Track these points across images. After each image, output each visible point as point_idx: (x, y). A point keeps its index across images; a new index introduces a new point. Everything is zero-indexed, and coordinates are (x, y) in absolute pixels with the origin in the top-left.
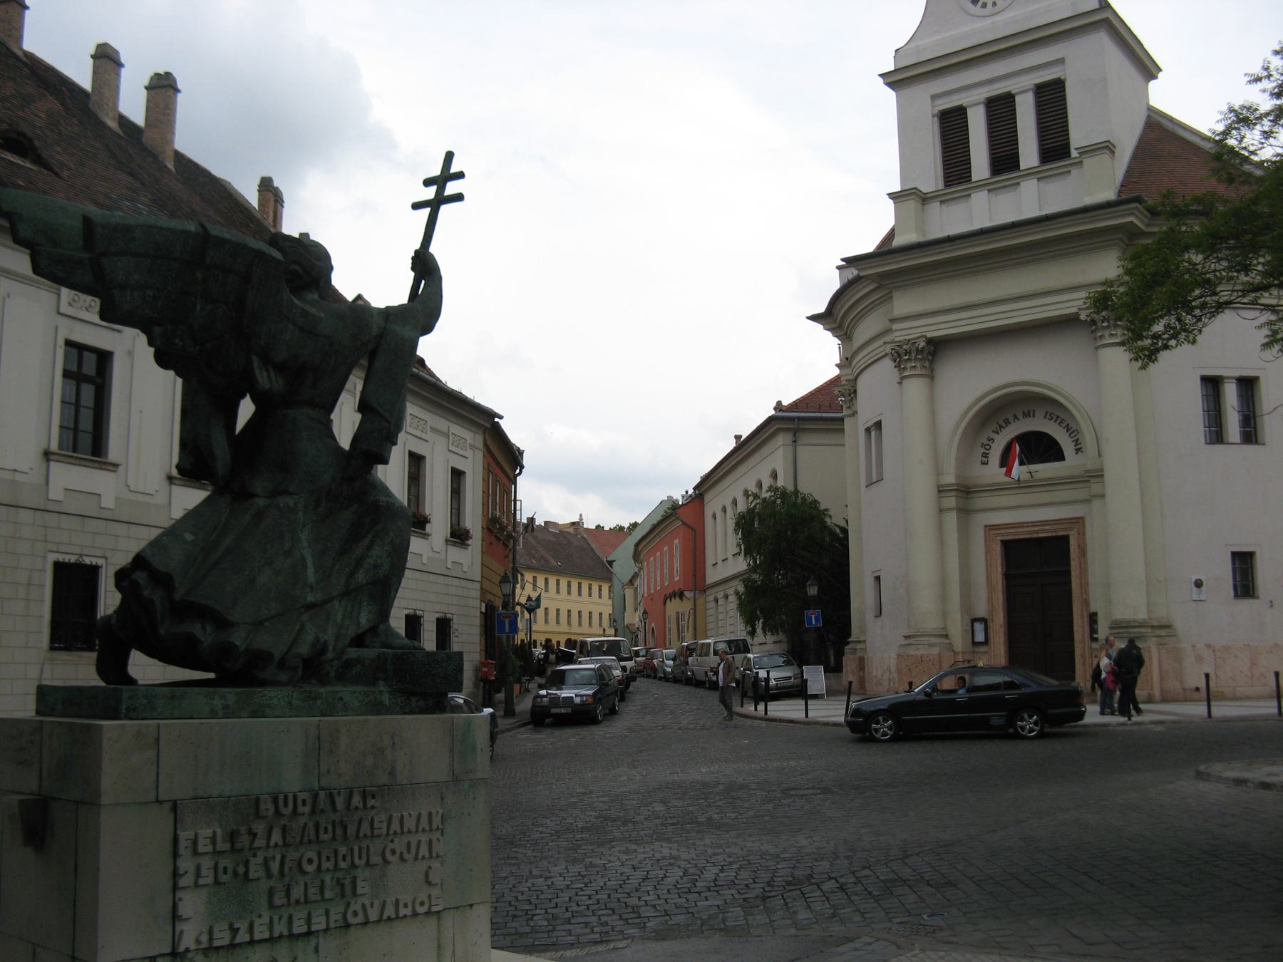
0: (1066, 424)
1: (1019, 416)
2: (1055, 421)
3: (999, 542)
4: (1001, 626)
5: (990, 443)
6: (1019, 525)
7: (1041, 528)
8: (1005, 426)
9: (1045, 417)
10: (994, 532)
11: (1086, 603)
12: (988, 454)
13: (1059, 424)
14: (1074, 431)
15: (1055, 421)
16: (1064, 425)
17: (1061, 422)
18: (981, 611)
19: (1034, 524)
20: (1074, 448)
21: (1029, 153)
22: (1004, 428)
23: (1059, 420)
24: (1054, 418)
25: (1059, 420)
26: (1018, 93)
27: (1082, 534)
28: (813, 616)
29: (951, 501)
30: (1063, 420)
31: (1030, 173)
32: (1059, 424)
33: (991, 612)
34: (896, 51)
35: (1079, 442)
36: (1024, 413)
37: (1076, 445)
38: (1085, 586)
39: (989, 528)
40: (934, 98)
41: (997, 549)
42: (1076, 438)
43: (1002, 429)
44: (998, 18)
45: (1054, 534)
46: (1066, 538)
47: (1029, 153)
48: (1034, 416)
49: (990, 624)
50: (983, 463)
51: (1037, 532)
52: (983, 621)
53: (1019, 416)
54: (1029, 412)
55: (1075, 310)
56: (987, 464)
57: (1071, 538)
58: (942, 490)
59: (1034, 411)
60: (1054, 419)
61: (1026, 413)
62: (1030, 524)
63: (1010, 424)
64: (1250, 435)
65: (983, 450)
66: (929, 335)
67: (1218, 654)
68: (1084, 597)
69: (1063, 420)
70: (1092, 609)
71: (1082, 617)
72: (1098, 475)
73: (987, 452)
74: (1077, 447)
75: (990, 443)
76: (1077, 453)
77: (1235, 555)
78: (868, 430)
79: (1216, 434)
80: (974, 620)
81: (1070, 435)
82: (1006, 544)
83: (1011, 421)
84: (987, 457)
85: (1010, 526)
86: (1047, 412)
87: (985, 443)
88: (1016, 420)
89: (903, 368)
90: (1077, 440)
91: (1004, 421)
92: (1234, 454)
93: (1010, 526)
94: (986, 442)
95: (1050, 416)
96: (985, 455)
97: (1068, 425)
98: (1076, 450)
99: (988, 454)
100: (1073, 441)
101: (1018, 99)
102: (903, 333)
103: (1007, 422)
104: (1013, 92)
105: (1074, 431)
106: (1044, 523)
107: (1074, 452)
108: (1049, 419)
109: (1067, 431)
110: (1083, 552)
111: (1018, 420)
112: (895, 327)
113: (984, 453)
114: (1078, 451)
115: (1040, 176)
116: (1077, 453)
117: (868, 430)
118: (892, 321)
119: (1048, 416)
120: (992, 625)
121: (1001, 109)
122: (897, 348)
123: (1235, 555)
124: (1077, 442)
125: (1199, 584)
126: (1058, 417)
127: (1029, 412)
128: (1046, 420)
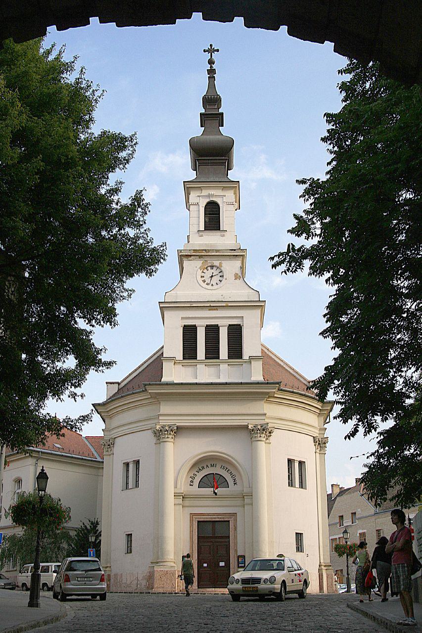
0: (230, 472)
1: (209, 466)
7: (217, 517)
10: (195, 517)
11: (236, 551)
19: (214, 514)
23: (227, 470)
25: (227, 470)
26: (221, 326)
27: (236, 520)
29: (180, 501)
38: (236, 544)
40: (182, 318)
44: (213, 291)
45: (222, 520)
46: (229, 521)
50: (191, 485)
51: (215, 518)
53: (209, 466)
55: (247, 424)
57: (230, 522)
64: (302, 485)
65: (191, 479)
66: (178, 424)
71: (234, 557)
72: (251, 495)
78: (127, 465)
79: (291, 484)
83: (205, 467)
89: (163, 438)
92: (296, 491)
95: (223, 467)
96: (192, 482)
102: (165, 421)
103: (203, 468)
110: (236, 529)
112: (160, 418)
114: (235, 484)
115: (229, 364)
117: (127, 465)
118: (159, 415)
119: (222, 467)
121: (212, 332)
122: (162, 428)
126: (227, 468)
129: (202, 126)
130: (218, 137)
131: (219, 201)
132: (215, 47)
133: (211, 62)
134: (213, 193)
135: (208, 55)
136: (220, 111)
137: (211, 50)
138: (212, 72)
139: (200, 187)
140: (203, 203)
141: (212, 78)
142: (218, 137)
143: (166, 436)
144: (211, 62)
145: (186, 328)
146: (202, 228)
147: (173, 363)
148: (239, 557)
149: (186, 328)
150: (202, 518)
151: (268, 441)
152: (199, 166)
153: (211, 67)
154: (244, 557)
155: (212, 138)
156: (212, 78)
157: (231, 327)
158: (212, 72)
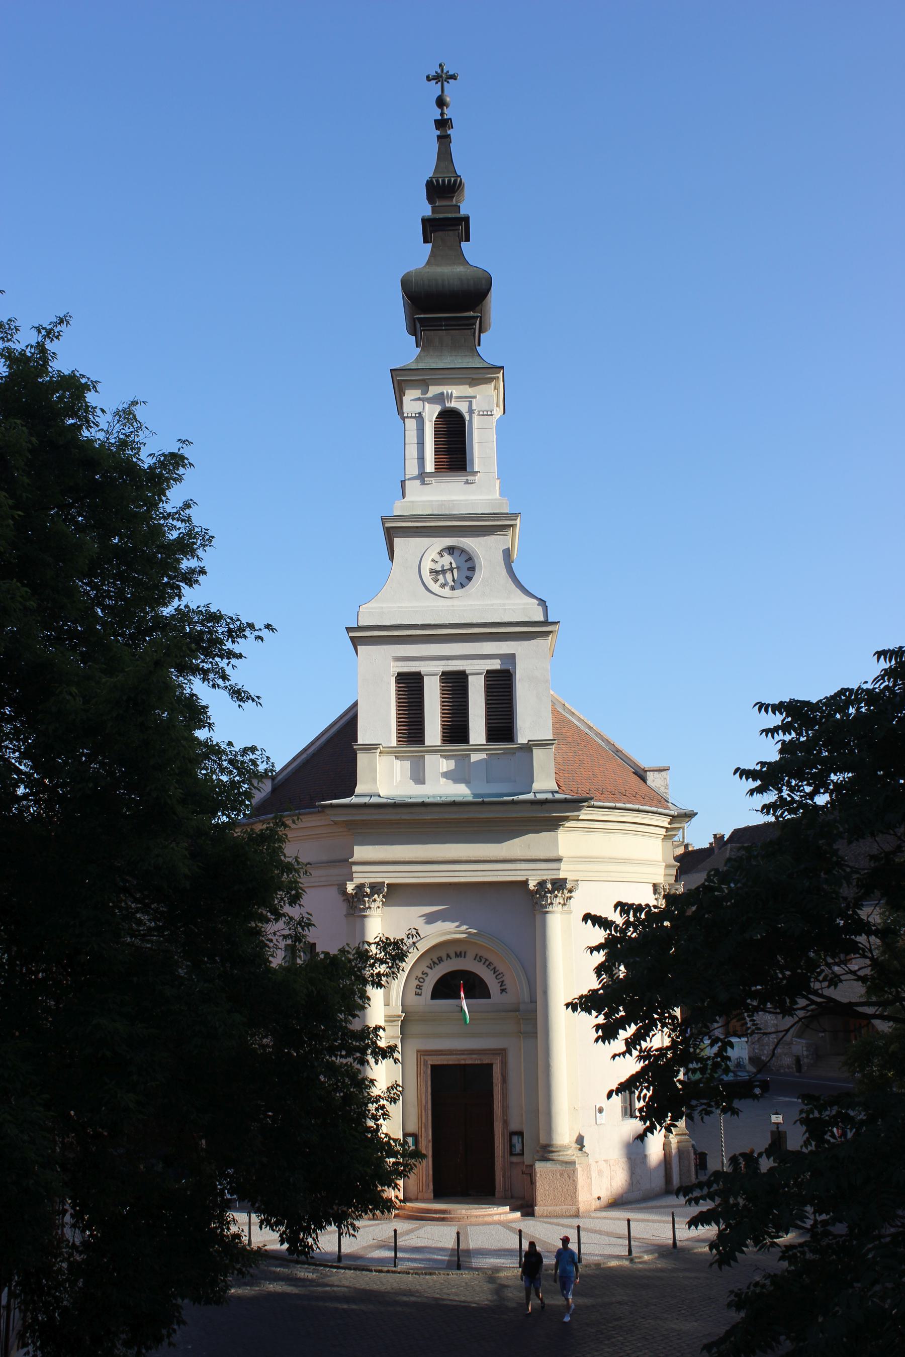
1: (452, 955)
3: (430, 1066)
4: (429, 1141)
5: (424, 976)
6: (449, 1052)
8: (438, 962)
9: (475, 959)
11: (506, 1123)
12: (422, 986)
13: (487, 966)
14: (500, 974)
15: (484, 964)
16: (492, 967)
20: (499, 988)
21: (478, 731)
22: (437, 964)
23: (487, 963)
24: (483, 960)
25: (487, 963)
27: (504, 1064)
30: (490, 963)
31: (478, 749)
32: (487, 966)
33: (420, 1128)
35: (504, 984)
36: (456, 953)
37: (501, 986)
38: (505, 1108)
42: (501, 980)
43: (436, 965)
44: (455, 602)
46: (490, 1066)
47: (478, 731)
48: (465, 957)
53: (452, 955)
54: (461, 953)
56: (421, 995)
59: (465, 953)
60: (483, 962)
61: (458, 954)
62: (459, 1052)
65: (417, 982)
67: (612, 1167)
68: (505, 1118)
69: (490, 963)
70: (514, 1126)
71: (503, 1135)
73: (421, 984)
74: (503, 987)
75: (424, 976)
76: (501, 993)
81: (496, 977)
82: (434, 1068)
83: (444, 957)
84: (421, 989)
85: (440, 1053)
86: (477, 955)
87: (419, 976)
90: (503, 982)
91: (438, 958)
93: (440, 1053)
94: (420, 975)
95: (479, 958)
97: (495, 968)
98: (501, 990)
99: (422, 986)
100: (499, 982)
101: (470, 678)
104: (467, 672)
105: (500, 974)
106: (471, 1052)
107: (500, 992)
109: (494, 973)
110: (504, 1080)
111: (451, 958)
113: (418, 985)
114: (503, 991)
116: (501, 993)
119: (478, 958)
124: (502, 983)
125: (601, 1110)
127: (461, 953)
128: (476, 961)
129: (426, 241)
130: (459, 269)
131: (463, 407)
132: (450, 69)
133: (441, 103)
134: (450, 392)
135: (434, 89)
136: (463, 212)
137: (441, 78)
138: (443, 124)
139: (424, 380)
140: (431, 413)
141: (444, 140)
142: (459, 269)
143: (367, 905)
144: (441, 103)
145: (401, 678)
146: (430, 467)
147: (378, 754)
148: (513, 1134)
149: (401, 678)
151: (566, 908)
152: (421, 331)
153: (442, 114)
154: (520, 1134)
155: (449, 272)
156: (444, 140)
157: (490, 674)
158: (443, 124)
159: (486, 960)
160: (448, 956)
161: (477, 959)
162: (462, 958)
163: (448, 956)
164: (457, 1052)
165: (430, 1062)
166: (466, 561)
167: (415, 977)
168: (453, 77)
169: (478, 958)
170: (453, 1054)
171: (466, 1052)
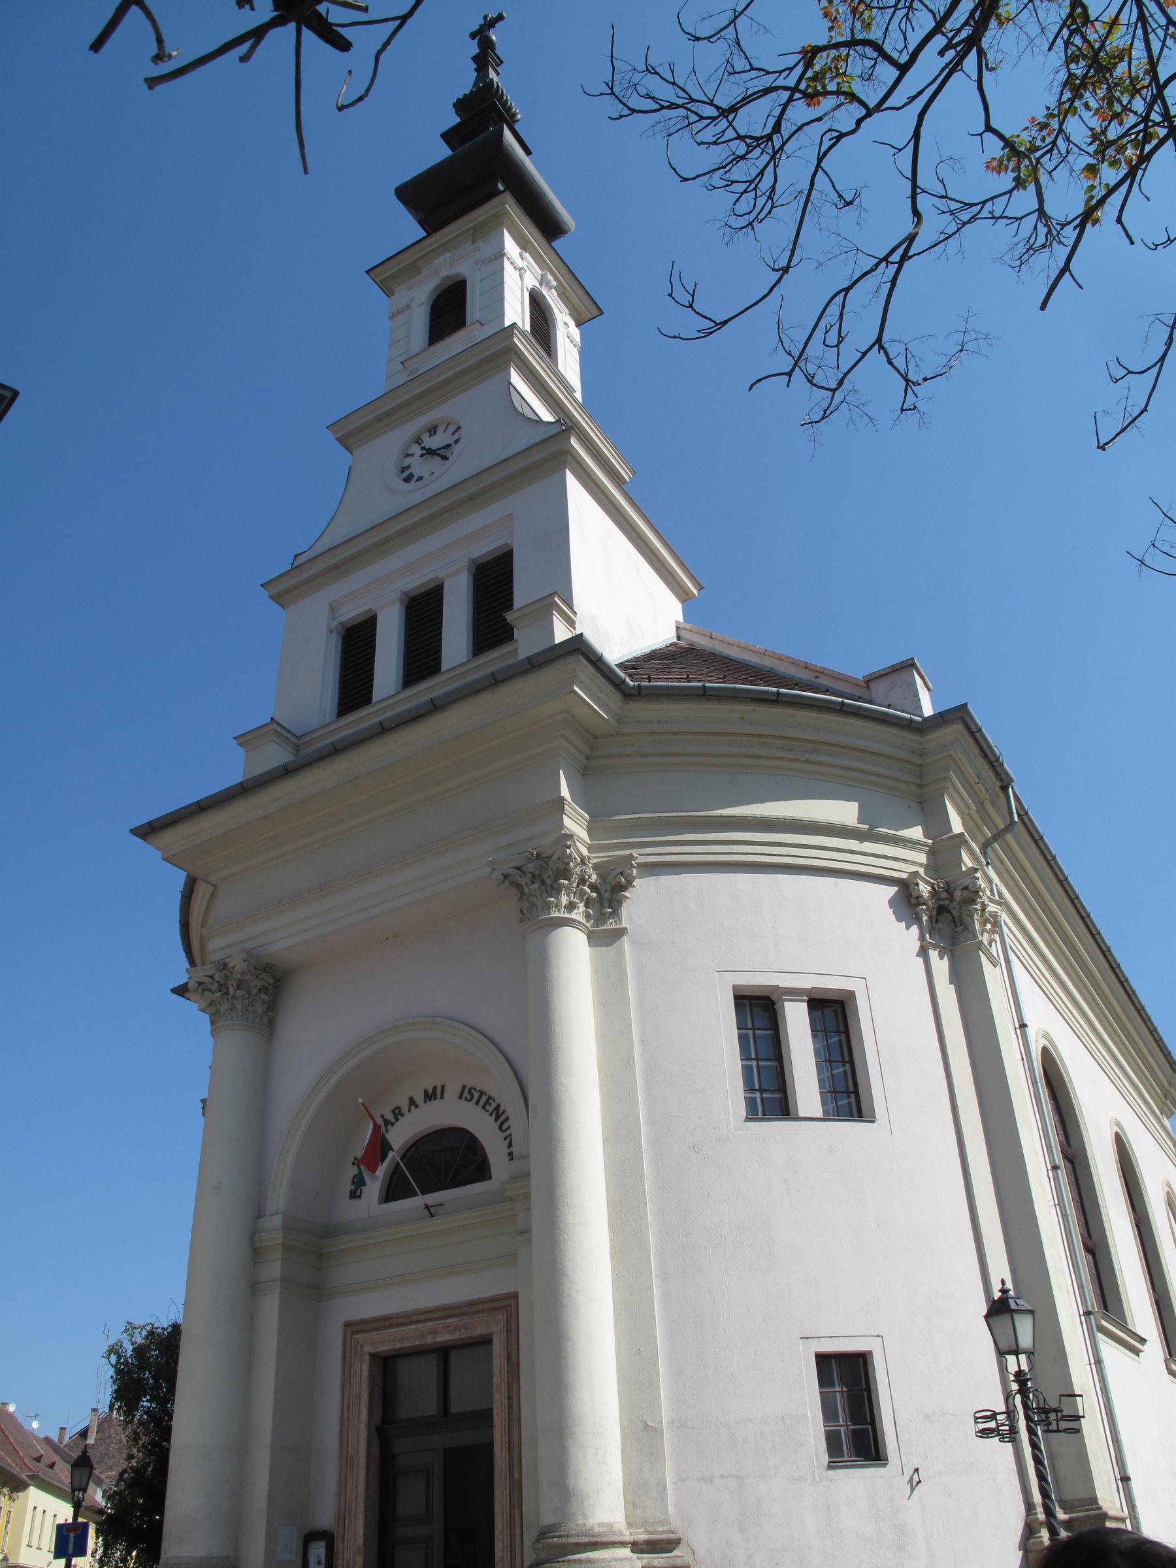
0: (494, 1105)
1: (419, 1099)
2: (477, 1103)
3: (367, 1357)
9: (460, 1097)
13: (484, 1107)
15: (477, 1103)
16: (490, 1108)
17: (487, 1103)
18: (325, 1518)
19: (430, 1314)
22: (393, 1124)
23: (484, 1099)
24: (476, 1095)
25: (484, 1099)
27: (512, 1330)
28: (72, 1535)
32: (484, 1107)
33: (343, 1516)
34: (295, 556)
39: (354, 1328)
41: (364, 1370)
43: (389, 1126)
48: (442, 1097)
49: (339, 1547)
52: (327, 1537)
53: (419, 1099)
54: (435, 1088)
58: (256, 1252)
59: (443, 1087)
61: (430, 1091)
62: (423, 1317)
63: (402, 1115)
69: (490, 1098)
77: (824, 1361)
80: (311, 1537)
81: (500, 1127)
83: (405, 1109)
85: (388, 1322)
86: (464, 1087)
88: (413, 1107)
91: (393, 1111)
93: (388, 1322)
95: (468, 1093)
103: (398, 1113)
104: (440, 576)
108: (466, 1099)
109: (496, 1120)
111: (417, 1106)
119: (466, 1094)
120: (341, 1547)
123: (824, 1361)
150: (385, 1341)
159: (482, 1093)
160: (412, 1102)
161: (464, 1098)
162: (438, 1101)
163: (412, 1102)
164: (418, 1318)
165: (368, 1349)
166: (444, 432)
167: (353, 1160)
168: (500, 17)
169: (466, 1094)
170: (412, 1323)
171: (437, 1315)
